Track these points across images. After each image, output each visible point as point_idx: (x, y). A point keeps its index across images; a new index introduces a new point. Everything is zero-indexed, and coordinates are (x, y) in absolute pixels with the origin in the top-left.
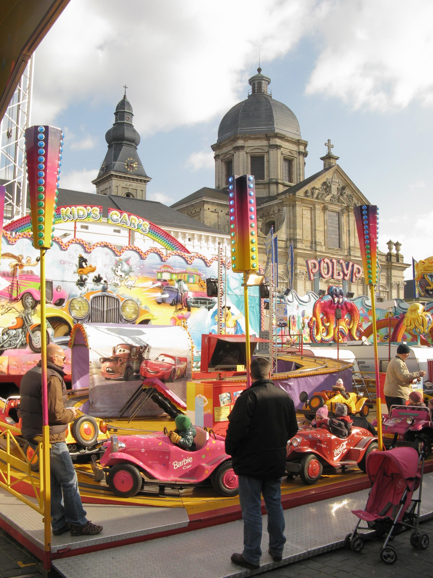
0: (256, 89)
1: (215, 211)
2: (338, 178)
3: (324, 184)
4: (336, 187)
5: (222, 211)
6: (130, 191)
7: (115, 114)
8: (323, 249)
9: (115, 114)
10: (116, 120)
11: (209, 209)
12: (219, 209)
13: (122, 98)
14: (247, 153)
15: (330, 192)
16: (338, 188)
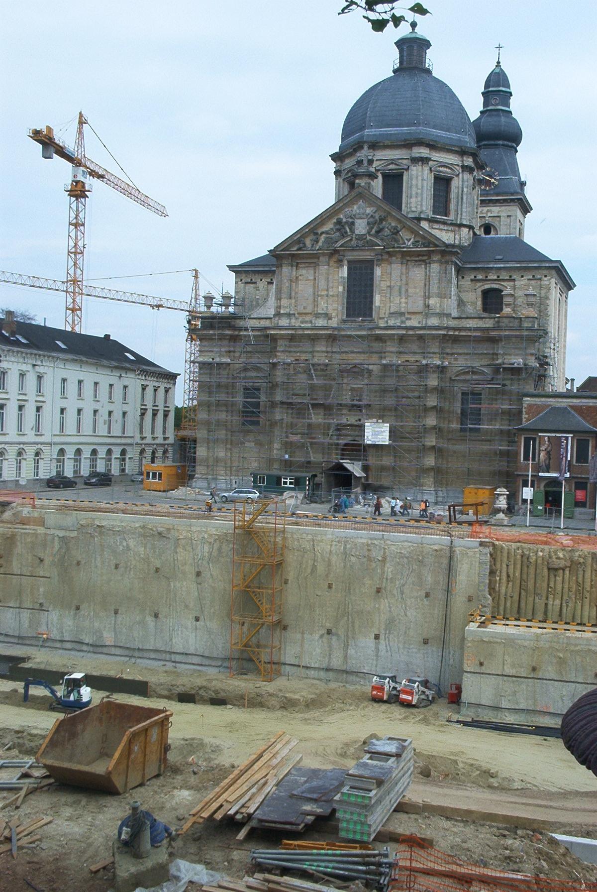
0: (405, 58)
1: (252, 282)
2: (371, 205)
3: (339, 222)
4: (365, 221)
5: (261, 280)
6: (488, 220)
7: (483, 94)
8: (334, 323)
9: (483, 94)
10: (485, 105)
11: (241, 280)
12: (256, 278)
13: (492, 67)
14: (344, 180)
15: (352, 231)
16: (368, 223)
